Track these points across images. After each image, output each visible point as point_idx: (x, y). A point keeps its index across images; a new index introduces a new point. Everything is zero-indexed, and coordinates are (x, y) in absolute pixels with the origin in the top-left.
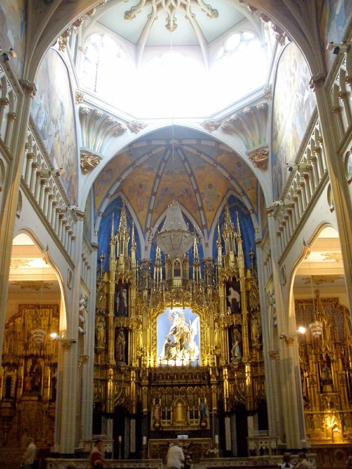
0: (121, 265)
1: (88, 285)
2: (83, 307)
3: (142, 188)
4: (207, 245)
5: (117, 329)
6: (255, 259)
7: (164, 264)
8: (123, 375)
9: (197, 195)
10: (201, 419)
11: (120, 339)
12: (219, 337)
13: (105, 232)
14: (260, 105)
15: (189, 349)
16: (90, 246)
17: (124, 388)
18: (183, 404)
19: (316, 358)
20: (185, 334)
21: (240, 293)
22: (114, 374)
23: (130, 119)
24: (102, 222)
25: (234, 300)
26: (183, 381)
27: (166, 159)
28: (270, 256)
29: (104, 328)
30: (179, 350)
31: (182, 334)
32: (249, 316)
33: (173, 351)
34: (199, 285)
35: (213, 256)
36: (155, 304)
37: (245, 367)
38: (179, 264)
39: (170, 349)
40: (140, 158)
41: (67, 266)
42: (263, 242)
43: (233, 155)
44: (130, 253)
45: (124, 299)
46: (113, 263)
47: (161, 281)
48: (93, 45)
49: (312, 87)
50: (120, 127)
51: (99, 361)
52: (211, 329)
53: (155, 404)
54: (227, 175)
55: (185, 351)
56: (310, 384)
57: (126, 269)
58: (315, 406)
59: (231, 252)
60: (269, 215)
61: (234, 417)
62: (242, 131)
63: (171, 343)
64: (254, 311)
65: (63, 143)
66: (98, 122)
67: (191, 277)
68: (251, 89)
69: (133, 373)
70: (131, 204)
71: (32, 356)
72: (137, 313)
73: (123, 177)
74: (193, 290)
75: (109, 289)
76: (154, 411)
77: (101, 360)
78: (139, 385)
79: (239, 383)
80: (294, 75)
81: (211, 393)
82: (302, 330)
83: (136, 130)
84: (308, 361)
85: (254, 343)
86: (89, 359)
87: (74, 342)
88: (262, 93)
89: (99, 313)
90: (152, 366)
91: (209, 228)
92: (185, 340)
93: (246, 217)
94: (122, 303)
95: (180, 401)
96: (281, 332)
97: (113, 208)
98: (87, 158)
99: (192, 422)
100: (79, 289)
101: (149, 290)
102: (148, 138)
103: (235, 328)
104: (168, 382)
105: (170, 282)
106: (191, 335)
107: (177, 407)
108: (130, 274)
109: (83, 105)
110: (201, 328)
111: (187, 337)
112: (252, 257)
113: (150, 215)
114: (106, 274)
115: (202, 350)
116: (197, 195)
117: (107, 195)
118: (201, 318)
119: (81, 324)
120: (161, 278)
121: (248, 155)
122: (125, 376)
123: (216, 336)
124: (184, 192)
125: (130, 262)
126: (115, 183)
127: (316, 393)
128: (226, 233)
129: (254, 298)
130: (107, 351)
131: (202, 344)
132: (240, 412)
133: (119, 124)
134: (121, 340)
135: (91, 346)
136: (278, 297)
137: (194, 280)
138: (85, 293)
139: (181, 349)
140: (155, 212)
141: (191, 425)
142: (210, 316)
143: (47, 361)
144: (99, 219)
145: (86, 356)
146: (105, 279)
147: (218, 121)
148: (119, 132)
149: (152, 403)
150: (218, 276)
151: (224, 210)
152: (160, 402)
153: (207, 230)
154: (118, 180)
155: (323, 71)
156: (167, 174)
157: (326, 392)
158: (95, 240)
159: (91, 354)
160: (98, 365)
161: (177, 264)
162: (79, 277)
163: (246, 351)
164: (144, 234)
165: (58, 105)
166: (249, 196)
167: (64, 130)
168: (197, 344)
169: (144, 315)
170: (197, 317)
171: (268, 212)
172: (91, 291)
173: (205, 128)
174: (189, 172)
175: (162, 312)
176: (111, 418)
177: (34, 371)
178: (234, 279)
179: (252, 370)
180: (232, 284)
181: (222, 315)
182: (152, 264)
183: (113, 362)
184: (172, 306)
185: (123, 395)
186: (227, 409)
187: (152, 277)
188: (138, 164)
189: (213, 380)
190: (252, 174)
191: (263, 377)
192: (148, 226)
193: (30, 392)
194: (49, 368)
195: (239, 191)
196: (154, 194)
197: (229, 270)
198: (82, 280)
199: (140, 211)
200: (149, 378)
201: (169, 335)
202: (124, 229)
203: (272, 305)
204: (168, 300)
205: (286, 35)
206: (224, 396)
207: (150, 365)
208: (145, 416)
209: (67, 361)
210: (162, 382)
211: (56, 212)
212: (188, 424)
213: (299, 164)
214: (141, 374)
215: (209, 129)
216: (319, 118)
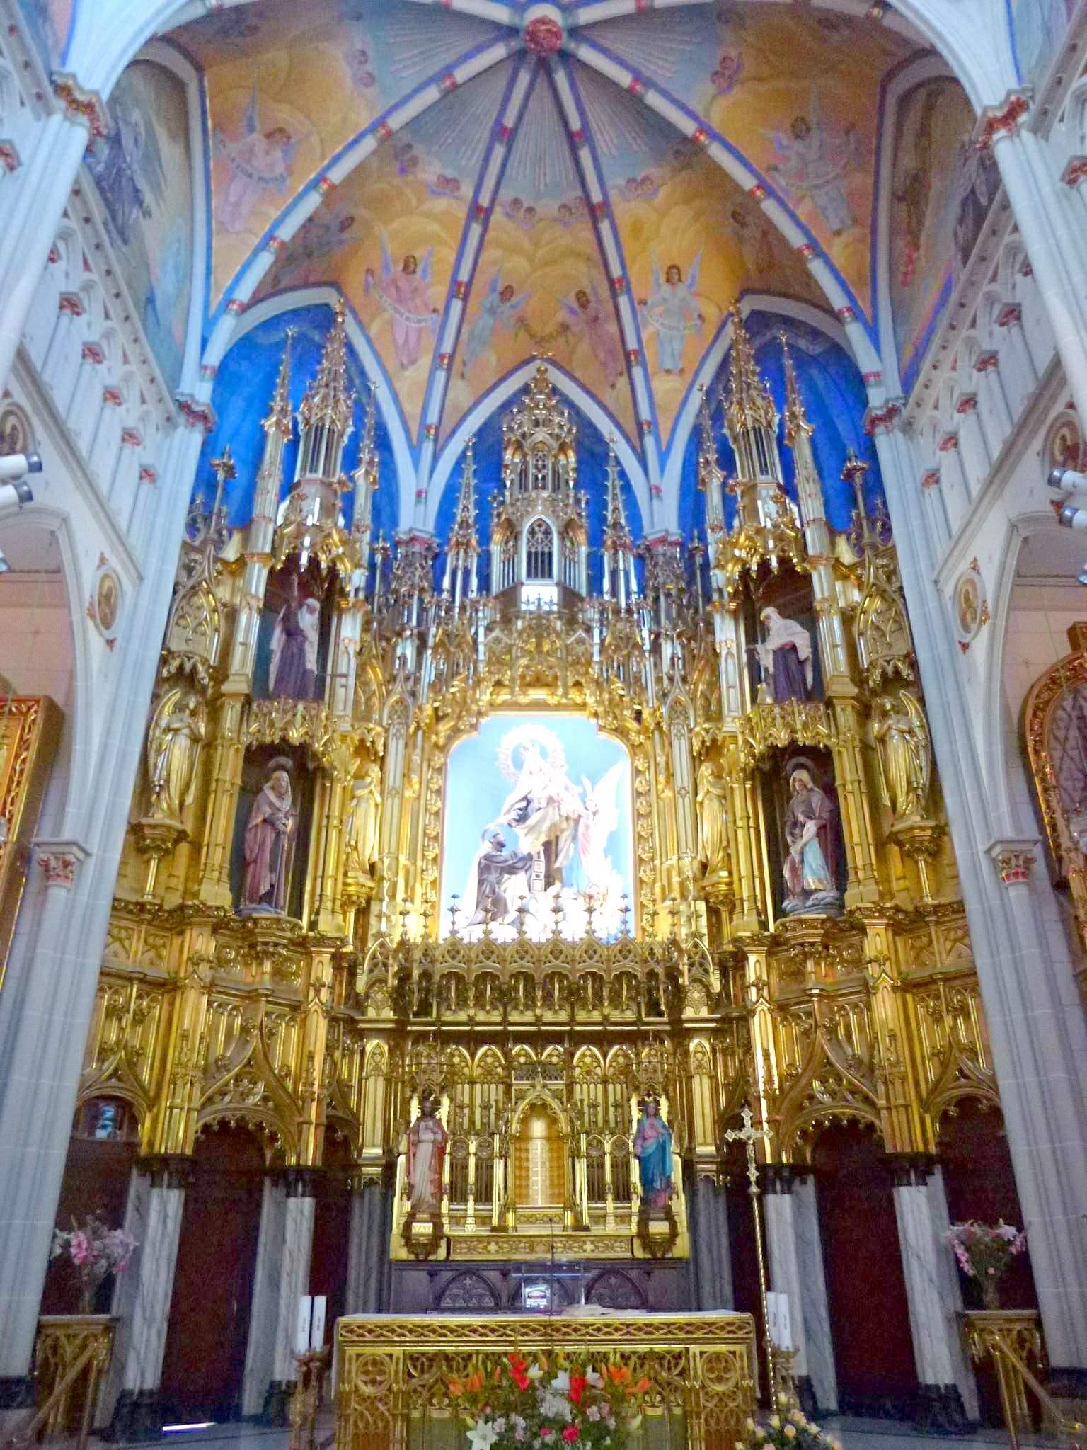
1: (135, 541)
4: (655, 492)
5: (260, 758)
6: (875, 484)
7: (485, 539)
8: (267, 966)
9: (623, 301)
10: (644, 1201)
11: (271, 804)
12: (718, 821)
16: (173, 408)
17: (269, 1035)
18: (553, 1121)
20: (564, 825)
26: (556, 1017)
29: (195, 739)
30: (539, 884)
31: (554, 826)
37: (863, 930)
38: (547, 532)
39: (499, 883)
45: (305, 638)
53: (419, 1119)
55: (567, 893)
59: (763, 478)
60: (1001, 133)
61: (809, 1191)
63: (505, 853)
76: (411, 1156)
78: (348, 1026)
81: (690, 1078)
90: (415, 935)
91: (664, 437)
94: (293, 656)
95: (538, 1109)
99: (600, 1219)
104: (488, 1018)
105: (510, 596)
106: (590, 822)
111: (574, 838)
114: (237, 537)
122: (278, 973)
123: (706, 813)
124: (573, 312)
126: (301, 197)
128: (742, 409)
135: (113, 805)
137: (607, 597)
139: (548, 884)
140: (463, 376)
141: (596, 1230)
142: (675, 743)
149: (406, 1112)
152: (443, 1113)
154: (314, 185)
159: (105, 848)
161: (540, 536)
164: (415, 451)
168: (616, 866)
169: (392, 731)
176: (169, 1186)
181: (731, 725)
183: (216, 893)
185: (254, 1068)
186: (776, 1153)
187: (437, 588)
189: (695, 1010)
191: (967, 978)
199: (403, 366)
200: (399, 998)
201: (501, 825)
206: (757, 1083)
208: (371, 1182)
210: (455, 1018)
212: (579, 1226)
214: (361, 985)
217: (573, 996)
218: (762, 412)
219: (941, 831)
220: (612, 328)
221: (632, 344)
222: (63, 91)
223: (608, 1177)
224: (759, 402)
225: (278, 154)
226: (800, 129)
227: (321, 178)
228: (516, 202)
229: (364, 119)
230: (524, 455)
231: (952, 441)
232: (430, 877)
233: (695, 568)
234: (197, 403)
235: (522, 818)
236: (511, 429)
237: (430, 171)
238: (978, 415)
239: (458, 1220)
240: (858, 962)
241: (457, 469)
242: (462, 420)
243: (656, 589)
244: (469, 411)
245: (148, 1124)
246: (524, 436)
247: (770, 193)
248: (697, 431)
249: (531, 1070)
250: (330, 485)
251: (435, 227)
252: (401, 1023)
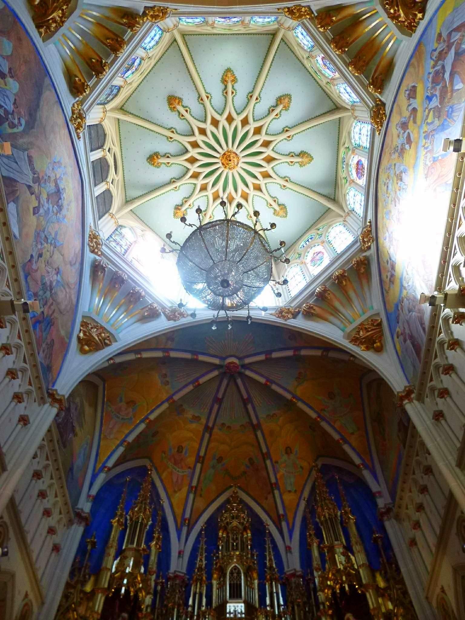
3: (182, 452)
4: (288, 549)
6: (388, 545)
7: (210, 578)
9: (268, 462)
16: (73, 515)
38: (239, 573)
48: (130, 229)
59: (336, 543)
70: (162, 481)
91: (291, 521)
114: (92, 579)
120: (204, 603)
128: (323, 509)
137: (268, 608)
153: (288, 524)
158: (85, 506)
161: (235, 575)
166: (354, 444)
172: (48, 601)
173: (278, 317)
199: (175, 492)
218: (332, 510)
220: (265, 474)
221: (273, 480)
222: (52, 395)
224: (330, 506)
226: (331, 396)
227: (146, 418)
229: (165, 396)
230: (228, 533)
231: (417, 525)
233: (310, 590)
234: (84, 513)
236: (221, 520)
237: (189, 414)
238: (426, 513)
241: (197, 541)
242: (200, 515)
243: (292, 603)
244: (204, 511)
246: (227, 523)
247: (323, 419)
248: (304, 519)
250: (139, 551)
251: (190, 435)
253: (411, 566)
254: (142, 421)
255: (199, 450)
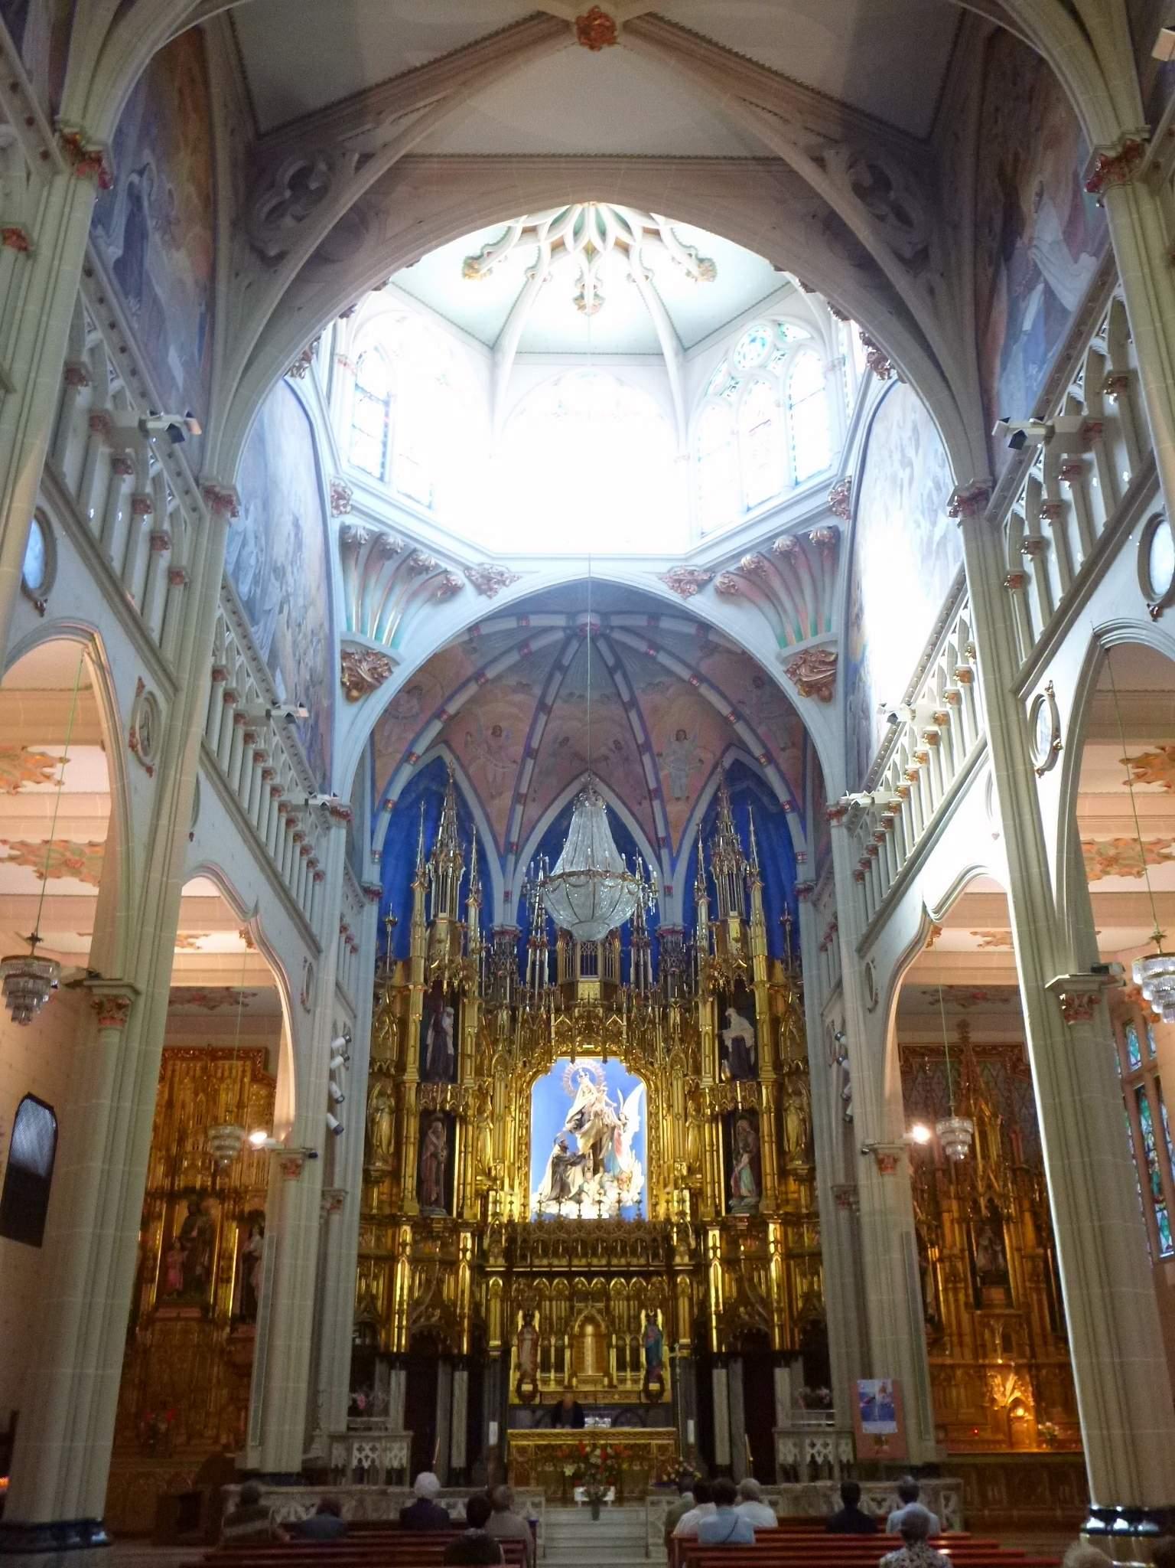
0: (440, 941)
2: (339, 1060)
7: (553, 941)
8: (439, 1243)
9: (646, 759)
10: (648, 1372)
13: (400, 853)
14: (817, 531)
15: (617, 1171)
17: (440, 1281)
18: (597, 1326)
19: (962, 1209)
21: (753, 1022)
22: (415, 1242)
23: (473, 559)
24: (392, 824)
25: (738, 1041)
26: (599, 1263)
27: (566, 662)
28: (834, 927)
29: (391, 1113)
30: (589, 1175)
32: (779, 1088)
33: (575, 1176)
34: (646, 998)
35: (684, 920)
36: (528, 1047)
39: (565, 1171)
40: (495, 660)
41: (303, 951)
42: (816, 890)
43: (745, 662)
44: (464, 910)
45: (446, 1033)
46: (419, 936)
47: (545, 986)
49: (954, 514)
50: (448, 580)
51: (375, 1203)
52: (676, 1117)
54: (726, 710)
55: (607, 1177)
56: (946, 1281)
57: (452, 953)
58: (961, 1344)
59: (732, 914)
61: (738, 1367)
62: (771, 596)
64: (790, 1074)
65: (299, 625)
66: (390, 566)
67: (625, 977)
68: (797, 483)
69: (467, 1239)
71: (189, 1191)
72: (479, 1072)
73: (452, 709)
74: (629, 1011)
75: (406, 1000)
77: (380, 1202)
78: (480, 1271)
79: (753, 1269)
80: (911, 464)
81: (675, 1298)
82: (921, 1134)
83: (491, 589)
84: (938, 1216)
85: (792, 1160)
86: (349, 1198)
87: (313, 1156)
88: (825, 498)
89: (377, 1073)
90: (516, 1218)
92: (607, 1145)
93: (774, 821)
94: (440, 1045)
95: (590, 1320)
96: (864, 1136)
97: (422, 787)
98: (360, 661)
99: (622, 1381)
100: (328, 1008)
101: (514, 1009)
102: (520, 609)
103: (742, 1117)
104: (560, 1264)
105: (570, 990)
107: (582, 1335)
108: (464, 968)
109: (350, 520)
110: (650, 1114)
111: (612, 1139)
112: (788, 928)
113: (519, 808)
115: (650, 1174)
116: (646, 759)
117: (409, 755)
118: (649, 1086)
119: (333, 1104)
120: (546, 978)
121: (784, 661)
122: (444, 1246)
125: (466, 935)
126: (428, 723)
127: (962, 1308)
128: (721, 861)
129: (793, 1039)
130: (396, 1175)
131: (650, 1159)
132: (754, 1356)
133: (446, 571)
134: (436, 1147)
136: (855, 1039)
138: (343, 1018)
139: (595, 1172)
141: (621, 1388)
143: (229, 1205)
144: (385, 818)
145: (339, 1191)
146: (398, 979)
147: (706, 571)
148: (444, 593)
150: (696, 974)
151: (715, 800)
152: (536, 1323)
153: (671, 854)
155: (983, 473)
156: (566, 702)
157: (990, 1306)
158: (372, 874)
159: (353, 1187)
160: (373, 1217)
162: (331, 979)
163: (769, 1181)
165: (287, 527)
166: (784, 767)
167: (300, 592)
168: (638, 1157)
170: (637, 1084)
171: (831, 816)
174: (626, 697)
175: (547, 1070)
177: (195, 1234)
178: (739, 983)
179: (785, 1234)
180: (736, 997)
182: (523, 940)
183: (412, 1208)
184: (573, 1055)
187: (523, 975)
188: (490, 674)
189: (682, 1260)
190: (791, 711)
191: (816, 1256)
192: (514, 838)
193: (180, 1294)
194: (234, 1225)
195: (758, 751)
196: (530, 753)
197: (725, 961)
198: (338, 985)
199: (493, 797)
200: (508, 1254)
202: (452, 845)
203: (839, 1063)
204: (564, 1036)
205: (892, 367)
207: (511, 1216)
208: (495, 1360)
209: (297, 1207)
210: (542, 1263)
211: (280, 810)
212: (611, 1385)
213: (913, 707)
214: (486, 1242)
215: (683, 591)
216: (969, 594)
217: (610, 1251)
219: (812, 1170)
223: (628, 1358)
225: (415, 702)
228: (571, 695)
232: (524, 1170)
235: (580, 1125)
239: (546, 1382)
240: (765, 1242)
242: (533, 828)
244: (538, 820)
245: (383, 1335)
247: (739, 716)
249: (587, 1296)
252: (509, 1268)
253: (815, 972)
254: (438, 715)
255: (530, 737)
